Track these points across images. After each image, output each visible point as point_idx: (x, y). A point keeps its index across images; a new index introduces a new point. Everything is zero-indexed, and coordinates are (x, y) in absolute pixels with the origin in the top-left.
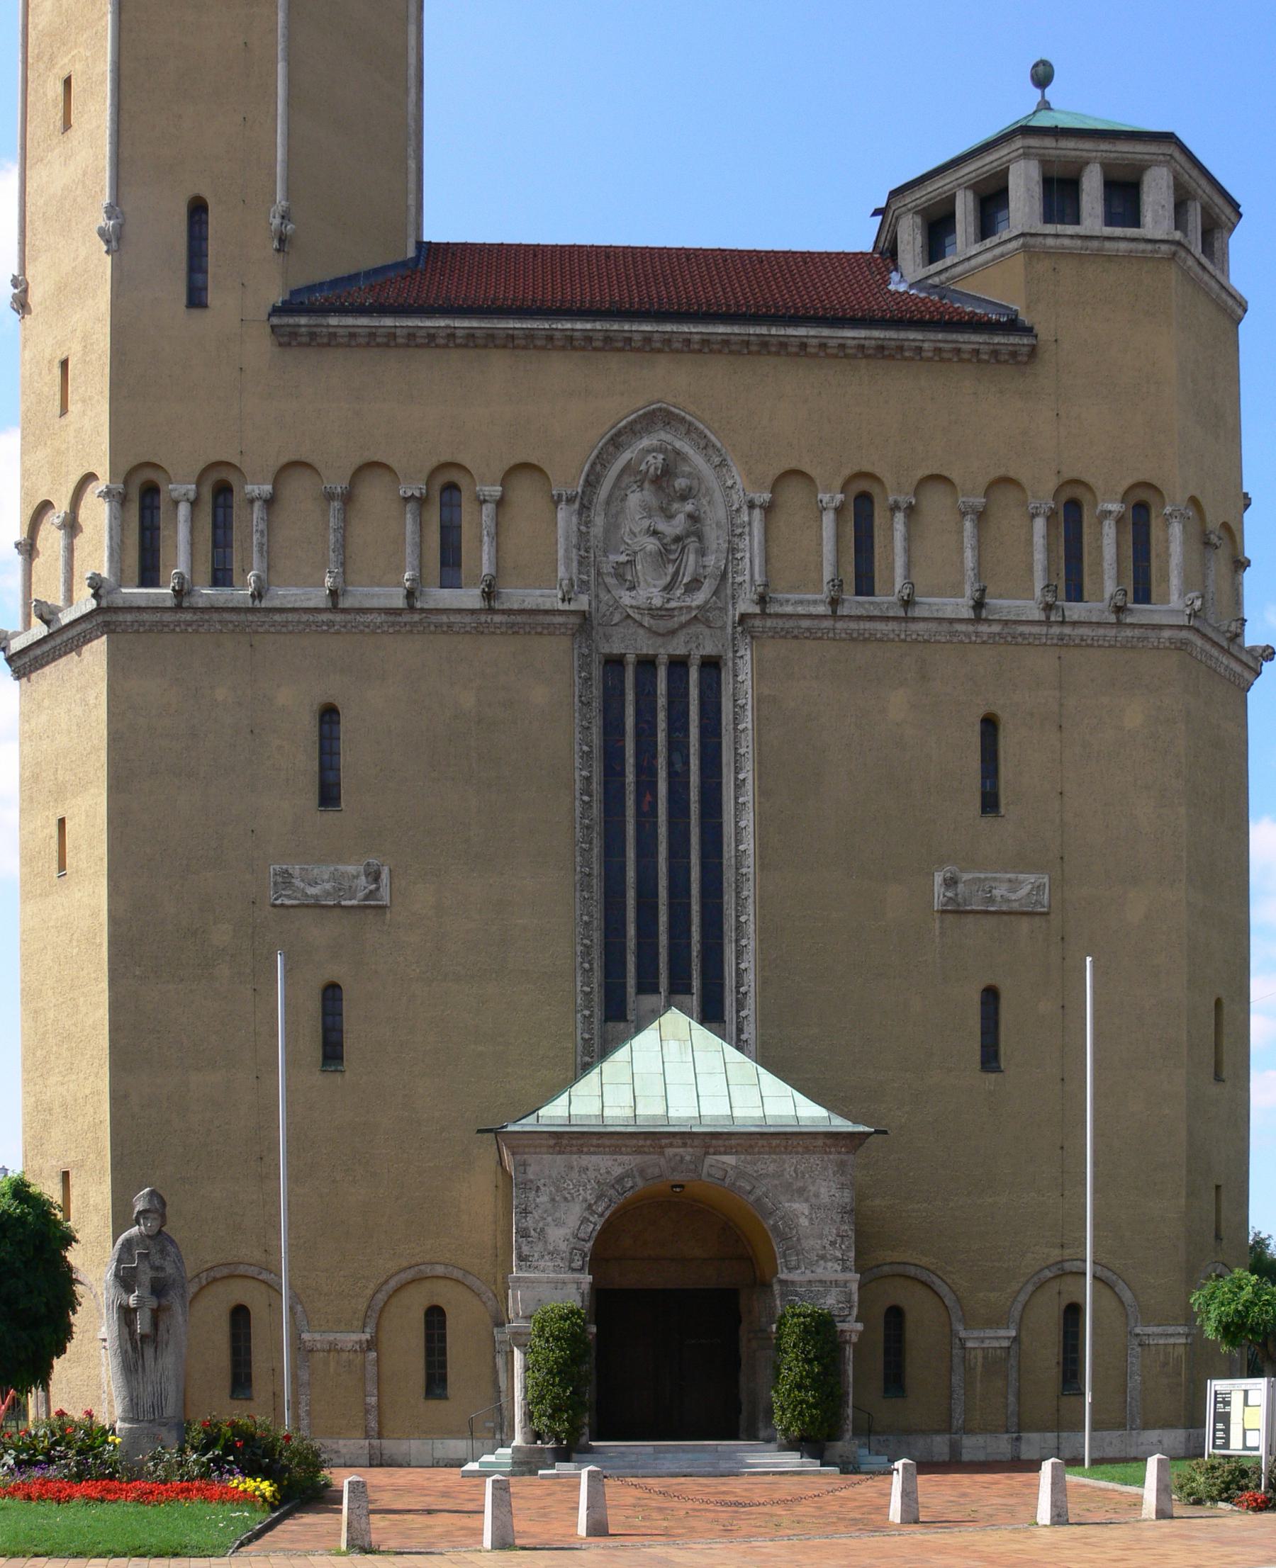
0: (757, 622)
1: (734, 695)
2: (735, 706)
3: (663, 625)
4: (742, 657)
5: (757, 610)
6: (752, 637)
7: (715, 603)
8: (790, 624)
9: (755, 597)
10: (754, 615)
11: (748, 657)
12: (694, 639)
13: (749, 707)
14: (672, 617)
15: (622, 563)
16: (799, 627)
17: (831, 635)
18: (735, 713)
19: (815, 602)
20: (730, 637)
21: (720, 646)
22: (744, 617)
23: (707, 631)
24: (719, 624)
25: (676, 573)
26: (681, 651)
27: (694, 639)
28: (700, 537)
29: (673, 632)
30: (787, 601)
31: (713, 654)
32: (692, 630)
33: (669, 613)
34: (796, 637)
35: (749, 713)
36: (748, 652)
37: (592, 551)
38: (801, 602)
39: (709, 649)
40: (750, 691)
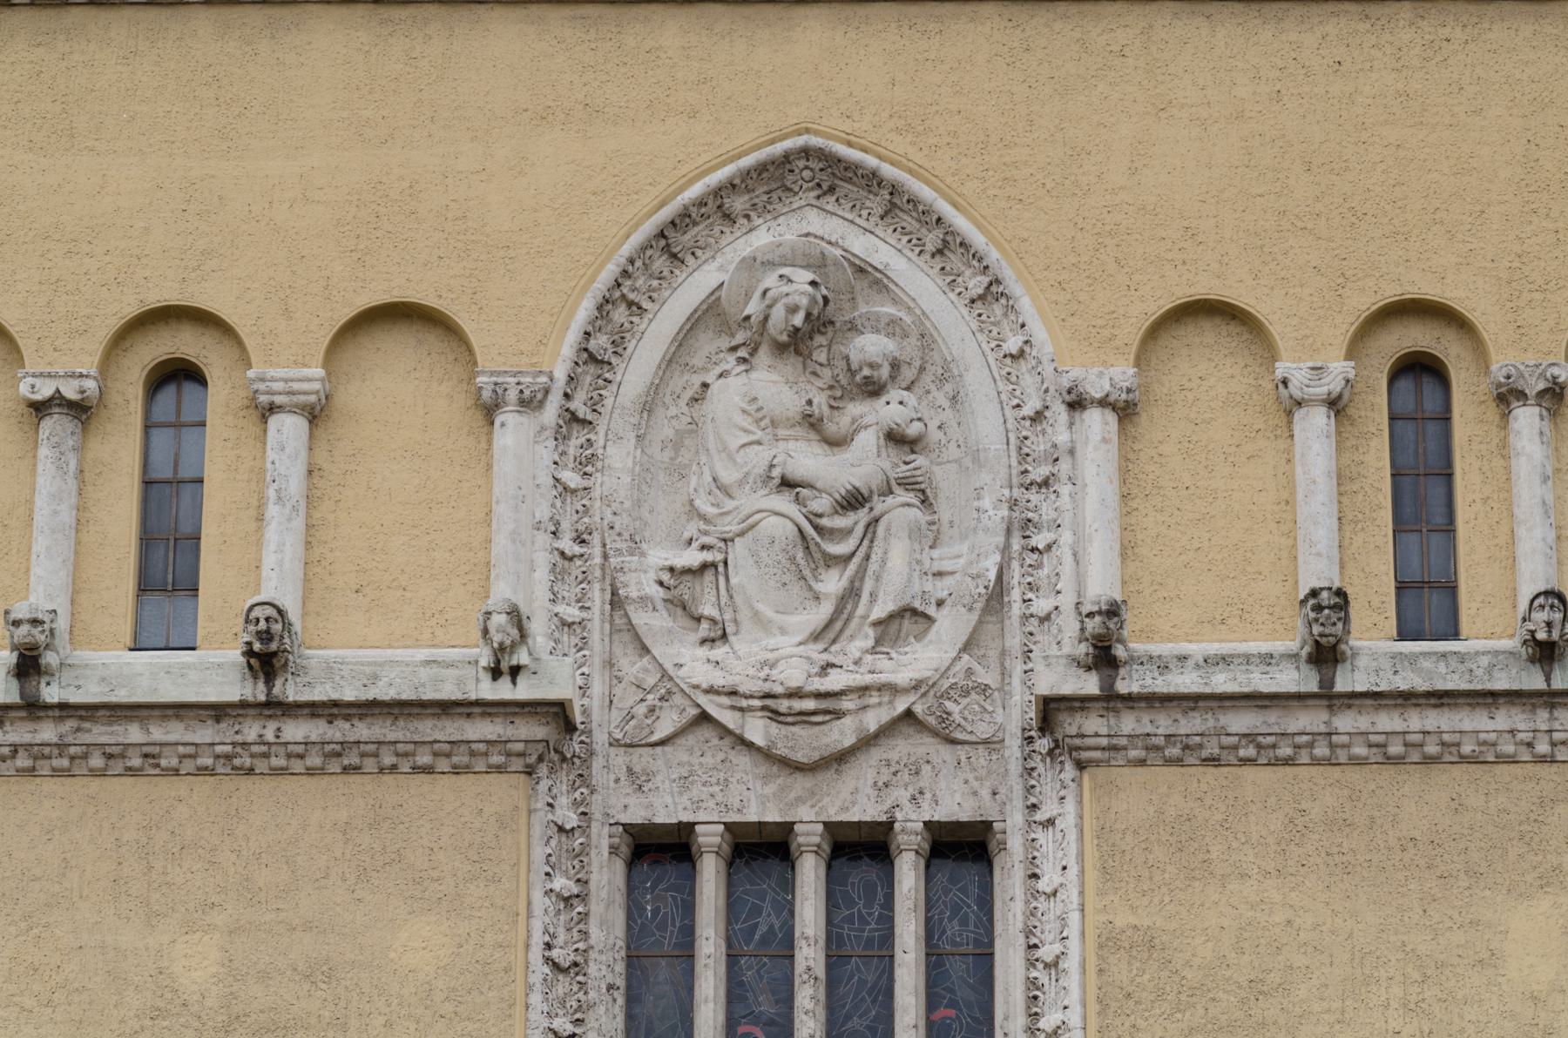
0: (1093, 724)
1: (1028, 932)
2: (1031, 963)
3: (805, 743)
4: (1050, 822)
5: (1090, 684)
6: (1081, 766)
7: (969, 672)
8: (1191, 724)
9: (1083, 649)
10: (1079, 703)
11: (1068, 822)
12: (905, 776)
13: (1071, 964)
14: (838, 714)
15: (688, 571)
16: (1222, 732)
17: (1321, 750)
18: (1032, 983)
19: (1267, 659)
20: (1015, 767)
21: (985, 793)
22: (1050, 709)
23: (944, 753)
24: (983, 730)
25: (851, 594)
26: (866, 810)
27: (905, 776)
29: (841, 758)
30: (1183, 658)
31: (964, 817)
32: (903, 747)
33: (829, 706)
34: (1213, 761)
35: (1073, 981)
36: (1070, 806)
37: (596, 539)
38: (1225, 660)
40: (1074, 917)
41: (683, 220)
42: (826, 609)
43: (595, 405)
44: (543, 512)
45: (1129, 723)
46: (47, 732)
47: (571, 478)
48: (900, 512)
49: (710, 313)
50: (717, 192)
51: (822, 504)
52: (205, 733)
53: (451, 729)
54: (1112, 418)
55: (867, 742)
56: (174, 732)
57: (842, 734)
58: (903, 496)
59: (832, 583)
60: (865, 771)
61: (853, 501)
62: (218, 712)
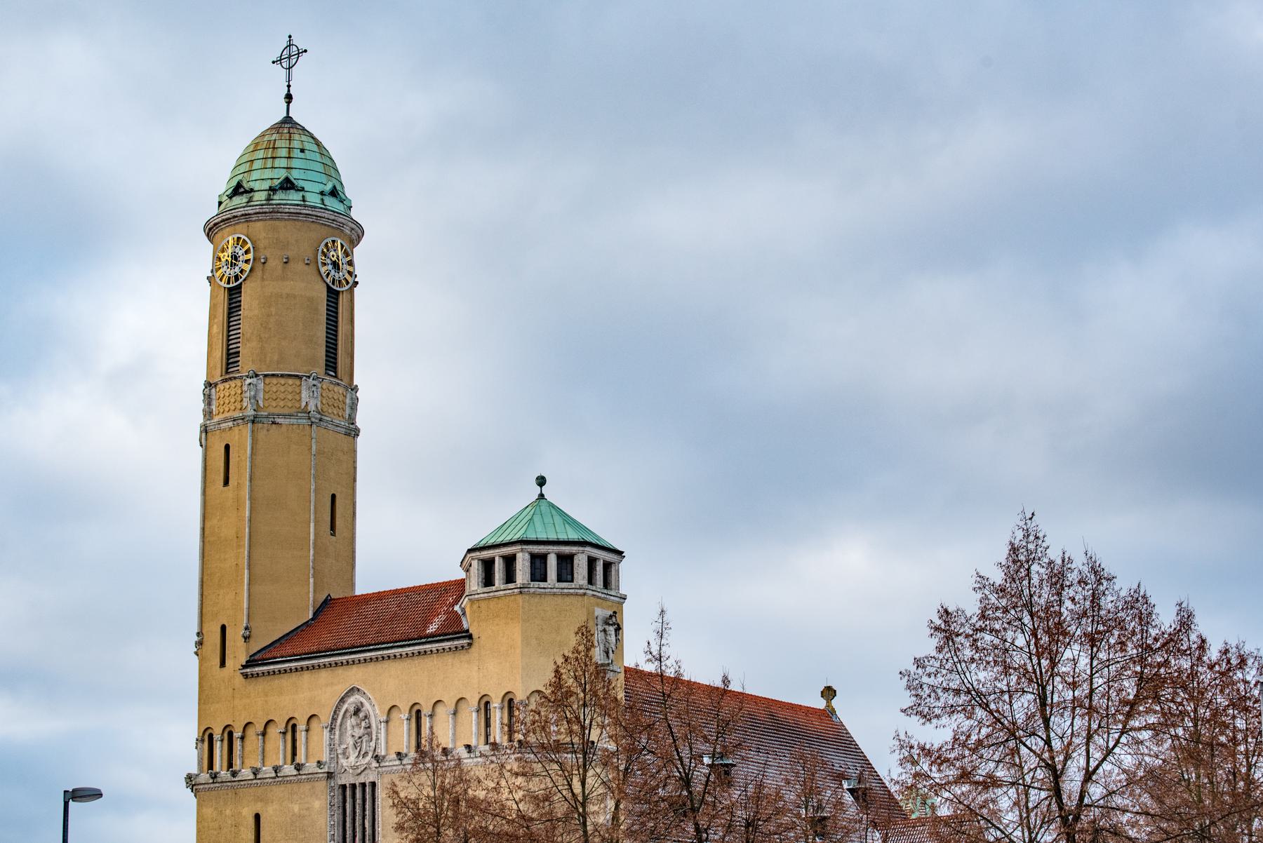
8: (390, 769)
26: (363, 781)
28: (370, 734)
32: (366, 772)
39: (372, 779)
41: (343, 698)
42: (357, 754)
43: (335, 726)
44: (328, 743)
45: (384, 769)
46: (280, 779)
47: (332, 737)
48: (365, 738)
49: (346, 711)
50: (347, 693)
51: (357, 738)
52: (295, 778)
53: (317, 775)
54: (385, 724)
55: (362, 772)
56: (291, 778)
57: (359, 771)
58: (366, 736)
59: (359, 749)
60: (363, 775)
61: (360, 738)
62: (295, 775)
